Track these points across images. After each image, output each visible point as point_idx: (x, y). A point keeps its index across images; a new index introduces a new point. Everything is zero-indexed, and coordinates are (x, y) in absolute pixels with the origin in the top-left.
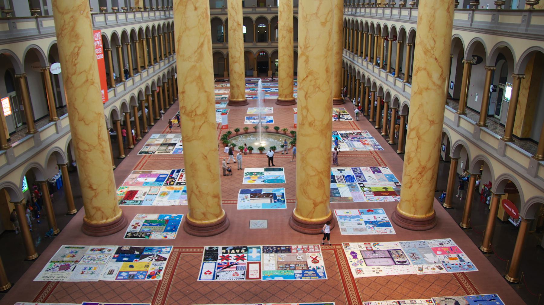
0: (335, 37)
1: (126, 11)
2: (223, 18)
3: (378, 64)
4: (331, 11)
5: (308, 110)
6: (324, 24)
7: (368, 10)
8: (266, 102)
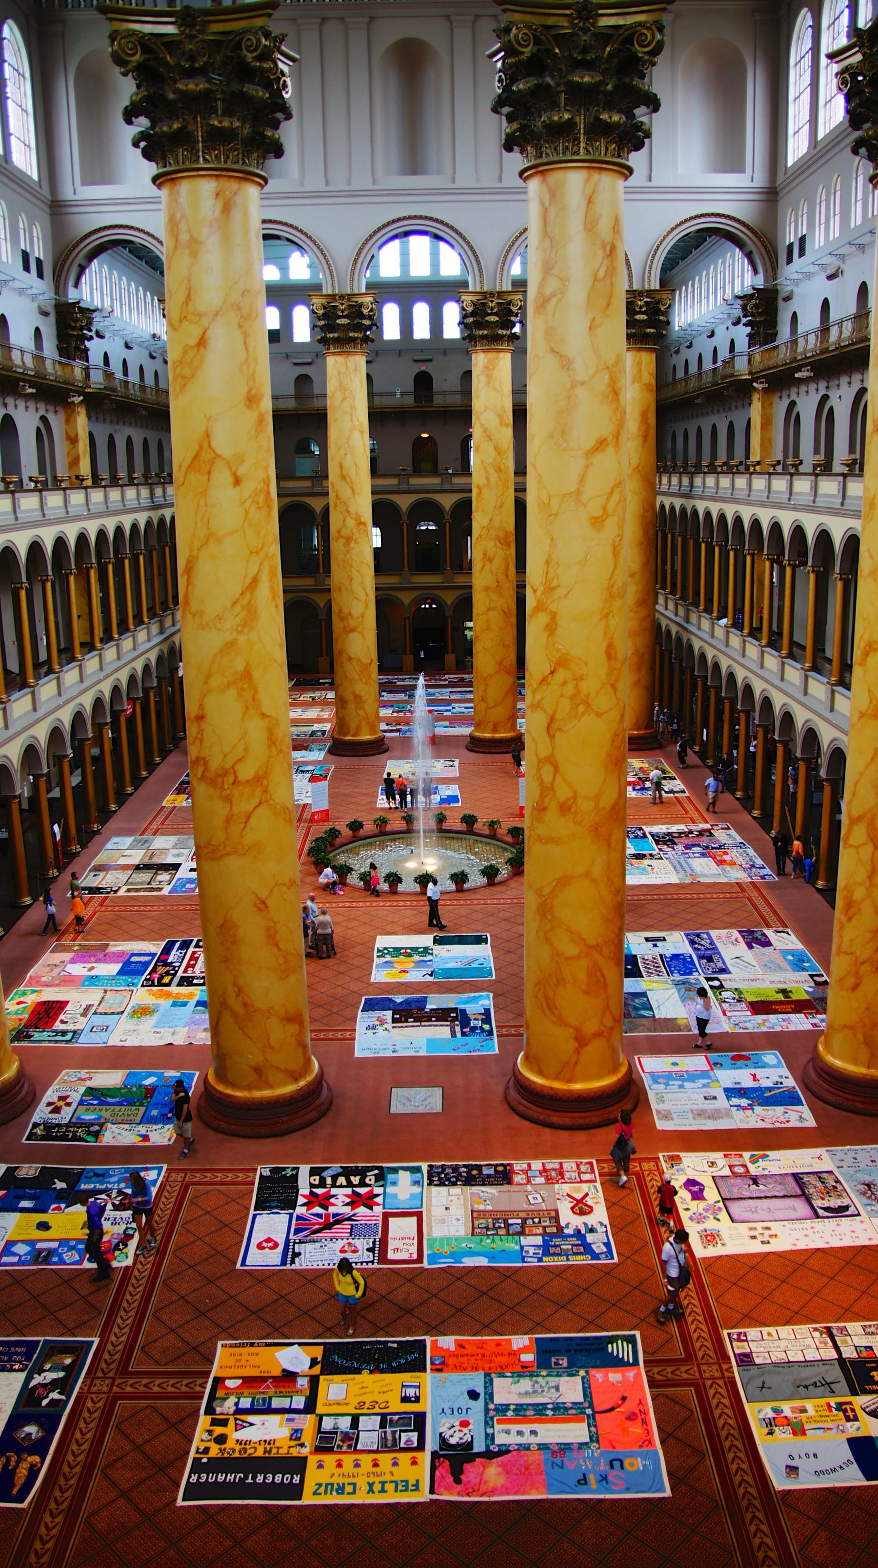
0: (632, 557)
1: (41, 488)
2: (317, 505)
3: (755, 633)
4: (619, 484)
5: (556, 768)
6: (597, 522)
7: (725, 481)
8: (439, 745)
